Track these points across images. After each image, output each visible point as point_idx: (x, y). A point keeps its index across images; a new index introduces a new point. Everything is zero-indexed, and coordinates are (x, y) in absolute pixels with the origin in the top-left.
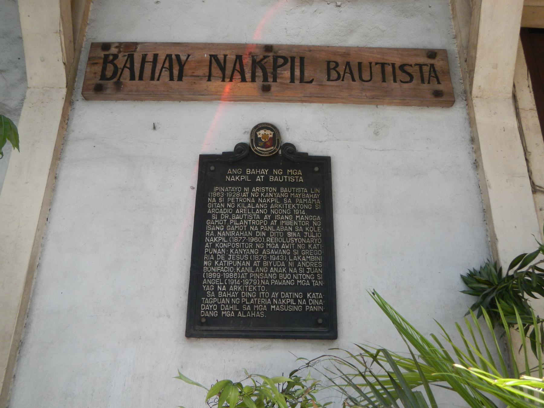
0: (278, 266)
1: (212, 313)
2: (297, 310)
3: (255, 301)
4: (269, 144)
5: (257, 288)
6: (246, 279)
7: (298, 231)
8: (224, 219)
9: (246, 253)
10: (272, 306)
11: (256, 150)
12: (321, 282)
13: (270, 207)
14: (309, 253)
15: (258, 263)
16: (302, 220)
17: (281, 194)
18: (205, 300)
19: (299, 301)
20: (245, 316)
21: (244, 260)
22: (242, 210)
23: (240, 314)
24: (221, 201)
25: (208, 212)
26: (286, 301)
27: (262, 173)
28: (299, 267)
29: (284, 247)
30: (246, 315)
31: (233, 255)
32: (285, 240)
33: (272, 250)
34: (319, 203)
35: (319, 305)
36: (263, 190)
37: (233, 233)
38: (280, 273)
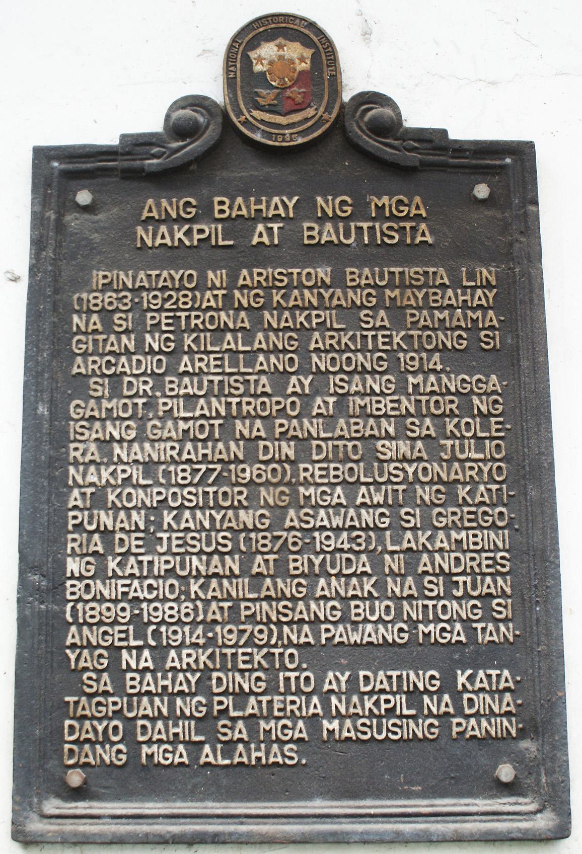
0: (345, 572)
1: (105, 752)
2: (420, 735)
3: (264, 705)
4: (296, 93)
5: (269, 656)
6: (228, 623)
7: (419, 438)
8: (136, 395)
9: (221, 526)
10: (325, 723)
11: (246, 123)
12: (508, 629)
13: (308, 344)
14: (461, 519)
15: (271, 563)
16: (433, 393)
17: (350, 293)
18: (76, 703)
19: (426, 699)
20: (227, 762)
21: (216, 551)
22: (201, 360)
23: (207, 756)
24: (121, 325)
25: (75, 370)
26: (377, 703)
27: (271, 213)
28: (426, 573)
29: (368, 501)
30: (231, 758)
31: (174, 535)
32: (368, 471)
33: (322, 512)
34: (495, 323)
35: (501, 715)
36: (282, 281)
37: (173, 448)
38: (355, 597)
